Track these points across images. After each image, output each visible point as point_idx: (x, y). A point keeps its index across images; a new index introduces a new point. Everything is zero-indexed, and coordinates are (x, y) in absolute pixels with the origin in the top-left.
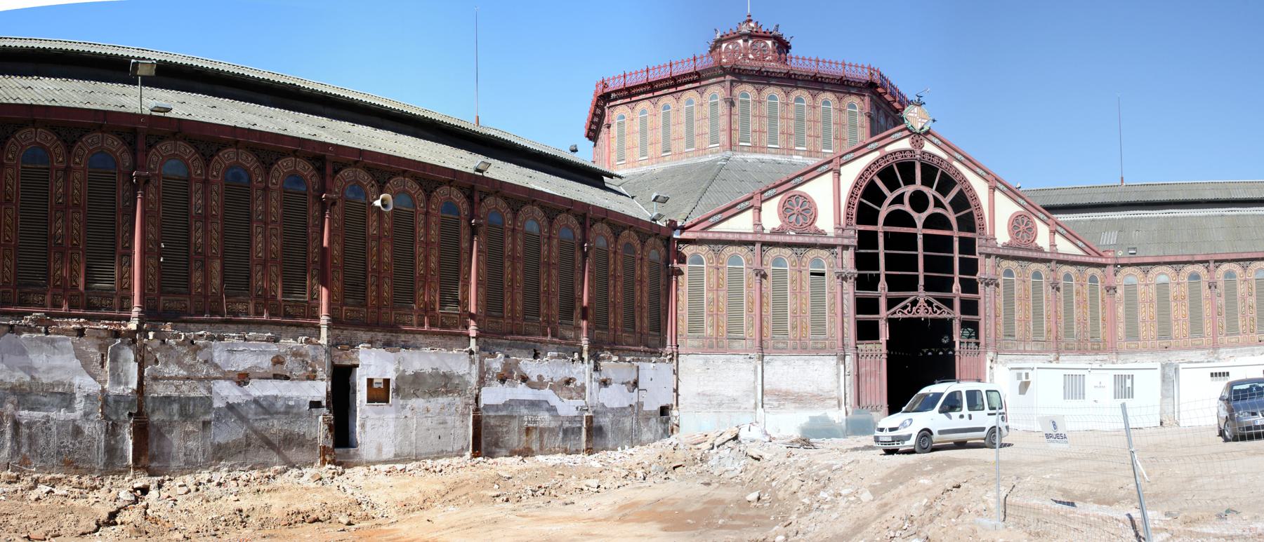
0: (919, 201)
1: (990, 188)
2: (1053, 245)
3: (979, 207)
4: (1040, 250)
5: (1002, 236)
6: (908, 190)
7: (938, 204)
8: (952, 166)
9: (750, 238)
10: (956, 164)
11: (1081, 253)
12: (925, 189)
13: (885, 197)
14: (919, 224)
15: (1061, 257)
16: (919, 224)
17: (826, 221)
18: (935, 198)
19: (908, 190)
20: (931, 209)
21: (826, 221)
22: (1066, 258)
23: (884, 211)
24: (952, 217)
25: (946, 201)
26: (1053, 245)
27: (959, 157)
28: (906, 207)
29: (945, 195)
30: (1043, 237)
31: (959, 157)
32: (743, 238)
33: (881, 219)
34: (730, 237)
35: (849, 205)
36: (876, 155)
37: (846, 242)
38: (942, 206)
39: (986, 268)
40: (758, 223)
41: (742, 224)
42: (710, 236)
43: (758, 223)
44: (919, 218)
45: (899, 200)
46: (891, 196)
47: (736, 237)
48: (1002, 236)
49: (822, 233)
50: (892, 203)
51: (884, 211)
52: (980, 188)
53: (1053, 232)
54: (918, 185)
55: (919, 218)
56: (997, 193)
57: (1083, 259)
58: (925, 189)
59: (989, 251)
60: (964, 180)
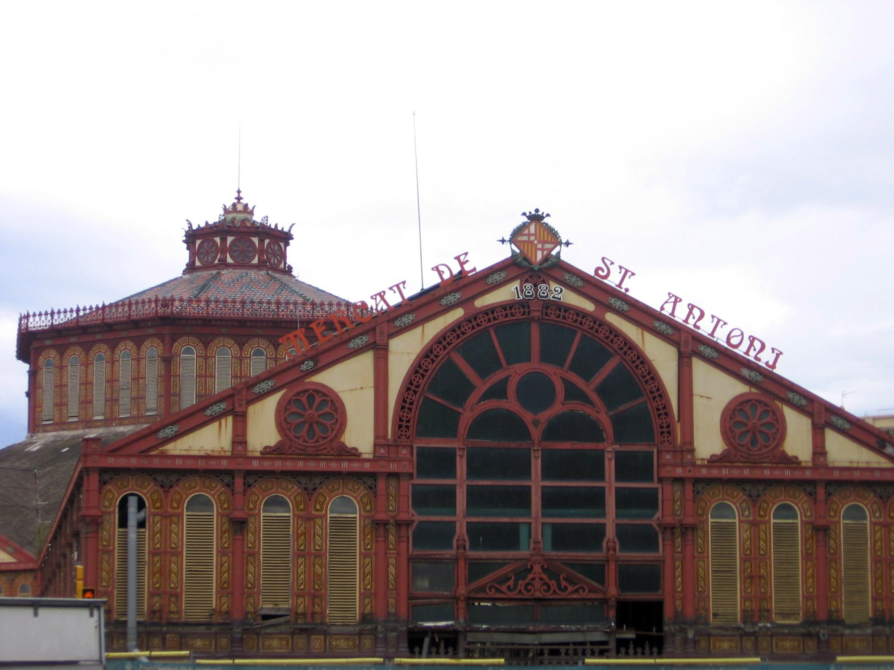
0: (536, 392)
1: (681, 356)
2: (819, 451)
3: (660, 392)
4: (792, 462)
5: (708, 441)
6: (516, 372)
7: (573, 393)
8: (603, 324)
9: (224, 464)
10: (611, 318)
11: (885, 463)
13: (471, 387)
14: (536, 433)
15: (836, 475)
16: (536, 433)
19: (516, 372)
20: (558, 408)
21: (359, 434)
22: (846, 476)
23: (468, 414)
24: (604, 418)
25: (589, 388)
26: (819, 451)
27: (618, 304)
28: (511, 404)
29: (587, 375)
30: (797, 437)
31: (618, 304)
32: (213, 464)
33: (463, 426)
34: (190, 464)
35: (404, 403)
36: (458, 314)
37: (393, 467)
39: (672, 505)
40: (240, 439)
41: (210, 440)
42: (156, 463)
45: (498, 391)
46: (482, 386)
47: (201, 465)
48: (708, 441)
49: (353, 454)
50: (486, 396)
51: (468, 414)
52: (661, 356)
54: (535, 365)
55: (537, 421)
58: (549, 369)
59: (679, 472)
60: (629, 346)
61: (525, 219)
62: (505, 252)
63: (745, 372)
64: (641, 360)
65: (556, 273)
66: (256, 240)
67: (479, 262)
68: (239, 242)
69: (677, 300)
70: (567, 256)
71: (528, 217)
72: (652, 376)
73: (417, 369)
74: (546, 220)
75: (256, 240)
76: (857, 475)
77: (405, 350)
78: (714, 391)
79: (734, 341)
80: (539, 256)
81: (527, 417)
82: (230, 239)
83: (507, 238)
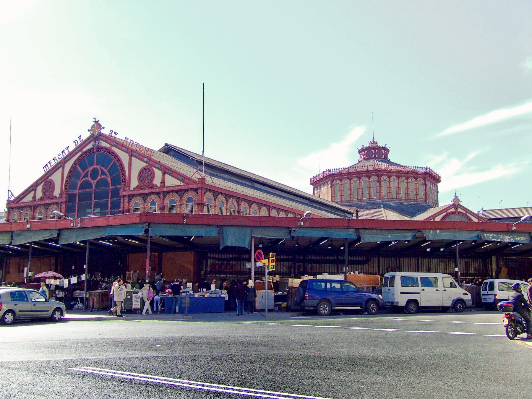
2: (163, 182)
3: (123, 170)
5: (134, 183)
9: (29, 204)
11: (182, 184)
12: (98, 167)
17: (57, 192)
18: (102, 170)
22: (171, 189)
25: (106, 171)
26: (163, 182)
36: (80, 154)
37: (62, 200)
38: (106, 175)
42: (18, 205)
43: (34, 197)
44: (94, 182)
48: (134, 183)
52: (124, 157)
53: (164, 174)
54: (95, 166)
56: (133, 158)
57: (186, 187)
58: (98, 167)
59: (124, 193)
61: (94, 123)
62: (88, 134)
63: (145, 159)
64: (119, 160)
65: (101, 137)
66: (373, 151)
67: (84, 138)
68: (374, 152)
69: (128, 139)
70: (103, 131)
71: (95, 122)
72: (121, 165)
73: (70, 172)
74: (99, 122)
75: (373, 151)
76: (174, 189)
77: (68, 166)
78: (138, 165)
79: (141, 149)
80: (97, 133)
81: (92, 181)
82: (366, 151)
83: (90, 129)
